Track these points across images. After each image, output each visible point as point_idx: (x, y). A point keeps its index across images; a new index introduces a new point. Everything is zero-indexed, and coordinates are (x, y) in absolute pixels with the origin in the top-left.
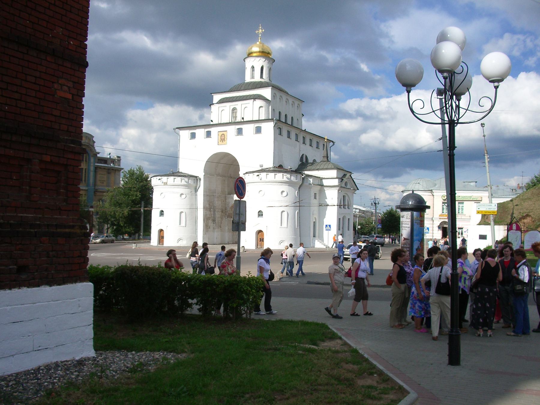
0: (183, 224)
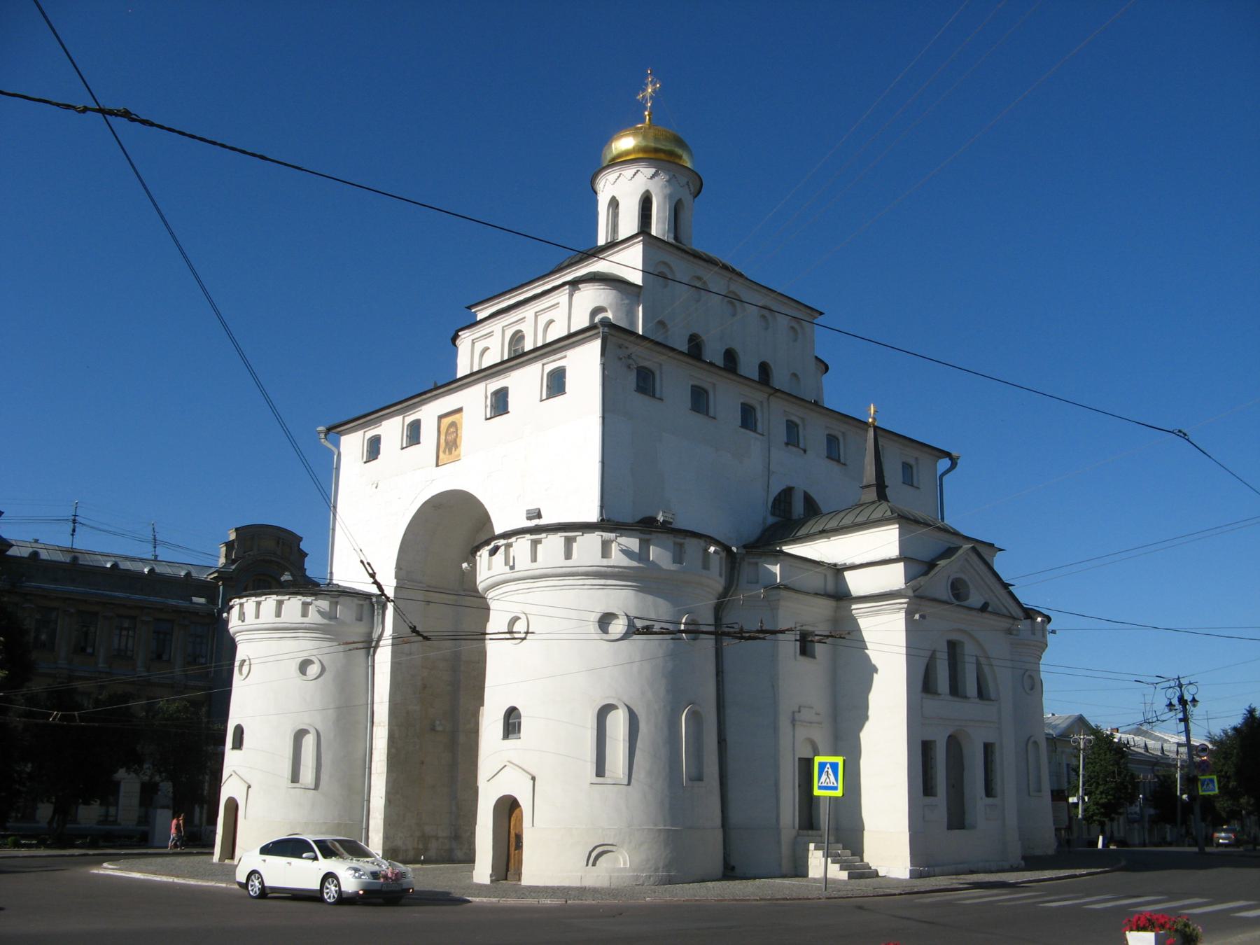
0: (307, 775)
